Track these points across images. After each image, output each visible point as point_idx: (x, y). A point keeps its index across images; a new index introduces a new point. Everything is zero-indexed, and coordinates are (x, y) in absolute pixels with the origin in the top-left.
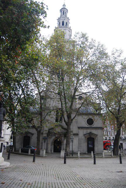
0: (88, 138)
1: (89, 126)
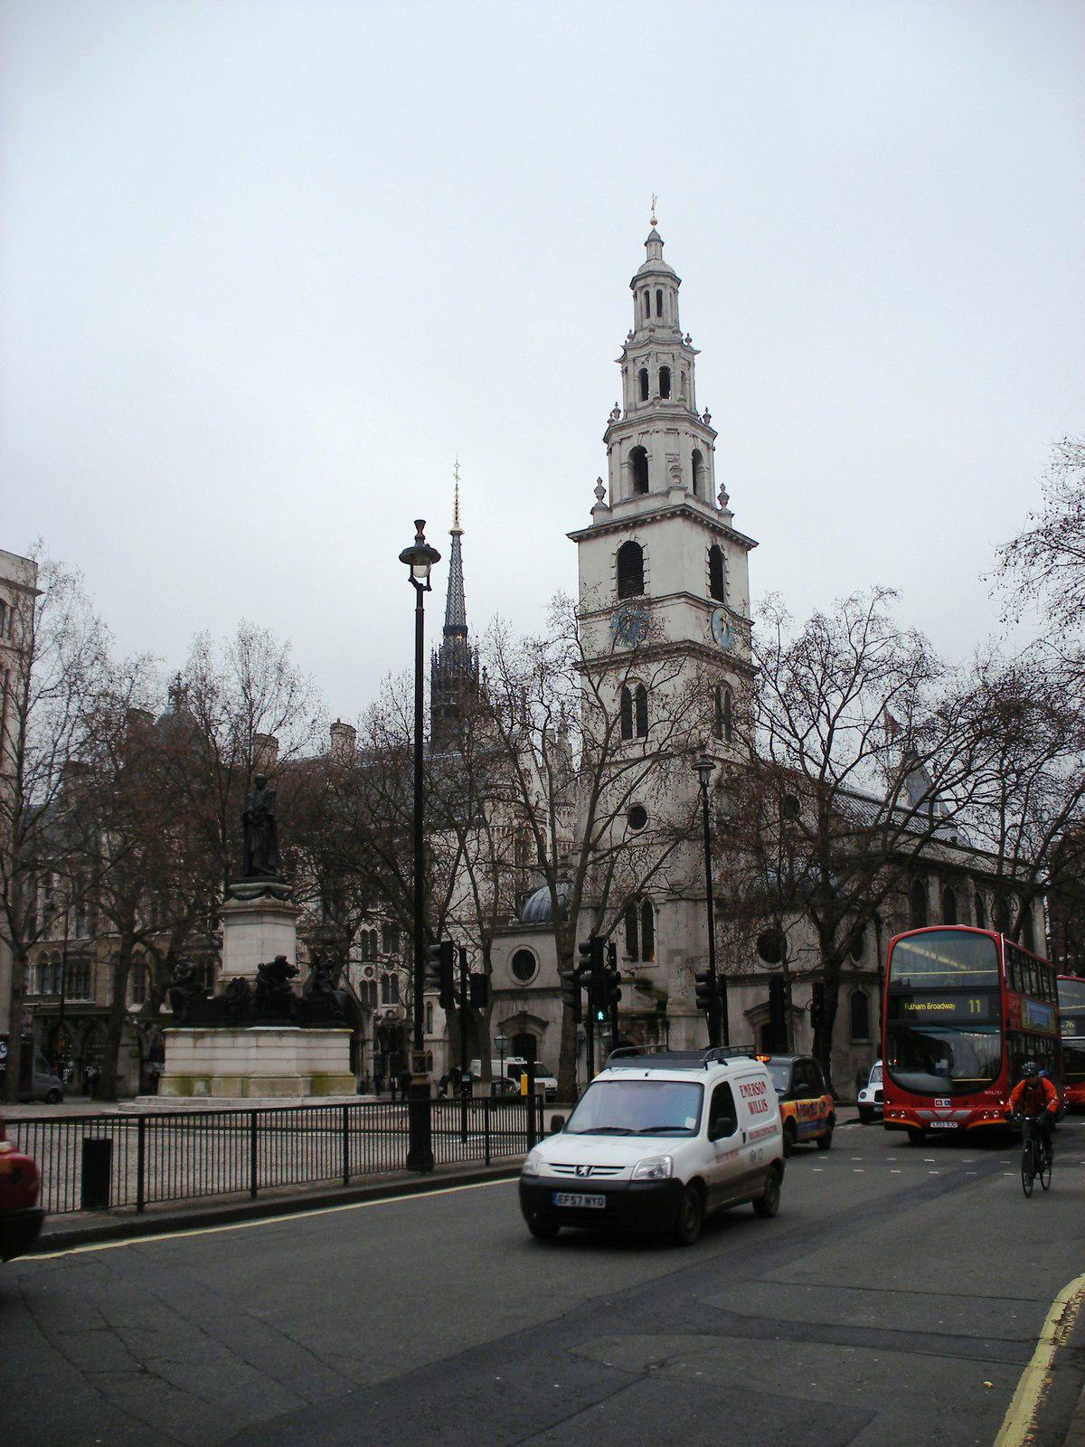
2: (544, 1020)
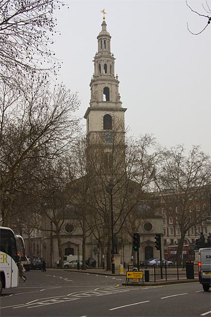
1: (146, 232)
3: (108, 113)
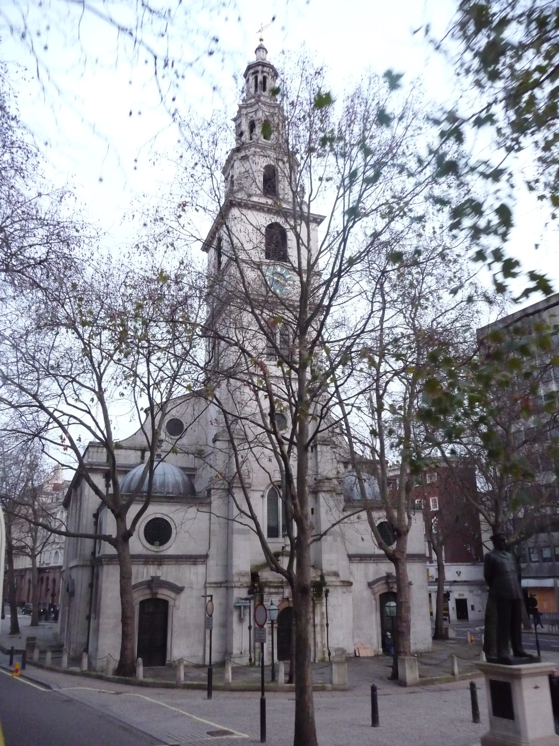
0: (381, 596)
2: (179, 584)
3: (280, 220)
